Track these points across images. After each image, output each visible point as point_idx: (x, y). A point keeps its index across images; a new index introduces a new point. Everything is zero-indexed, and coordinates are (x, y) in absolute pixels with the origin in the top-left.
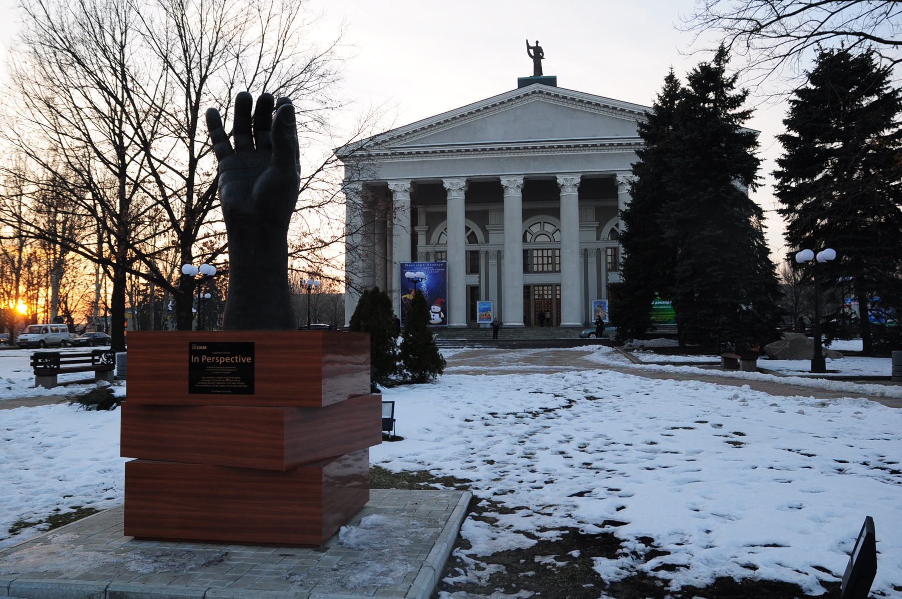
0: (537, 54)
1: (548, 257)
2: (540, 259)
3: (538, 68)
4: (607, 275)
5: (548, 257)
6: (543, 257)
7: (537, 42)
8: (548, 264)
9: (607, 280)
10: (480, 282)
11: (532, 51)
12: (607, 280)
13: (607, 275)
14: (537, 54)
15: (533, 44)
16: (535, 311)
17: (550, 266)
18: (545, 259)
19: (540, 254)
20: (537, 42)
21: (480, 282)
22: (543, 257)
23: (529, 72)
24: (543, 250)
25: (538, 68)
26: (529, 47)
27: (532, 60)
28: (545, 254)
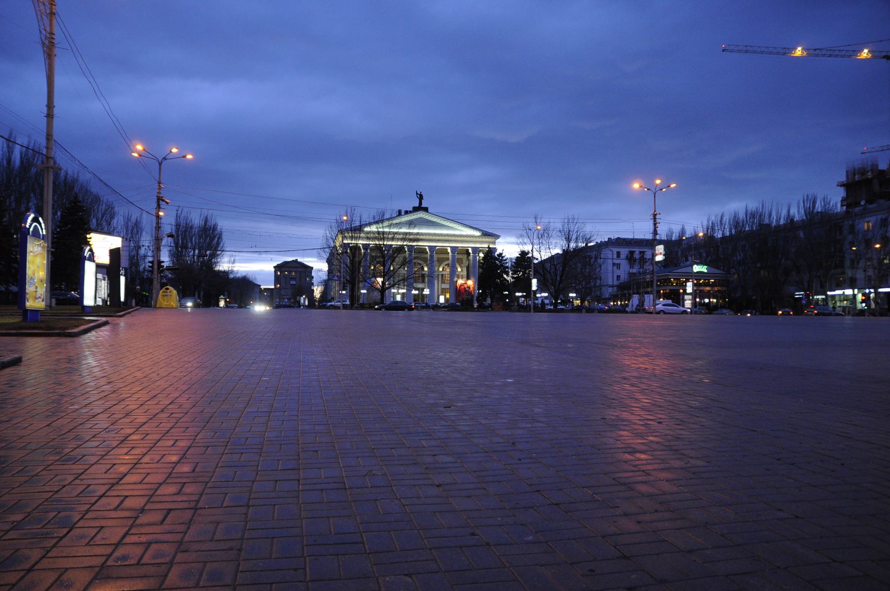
0: (421, 197)
3: (420, 203)
14: (421, 197)
23: (417, 205)
25: (420, 203)
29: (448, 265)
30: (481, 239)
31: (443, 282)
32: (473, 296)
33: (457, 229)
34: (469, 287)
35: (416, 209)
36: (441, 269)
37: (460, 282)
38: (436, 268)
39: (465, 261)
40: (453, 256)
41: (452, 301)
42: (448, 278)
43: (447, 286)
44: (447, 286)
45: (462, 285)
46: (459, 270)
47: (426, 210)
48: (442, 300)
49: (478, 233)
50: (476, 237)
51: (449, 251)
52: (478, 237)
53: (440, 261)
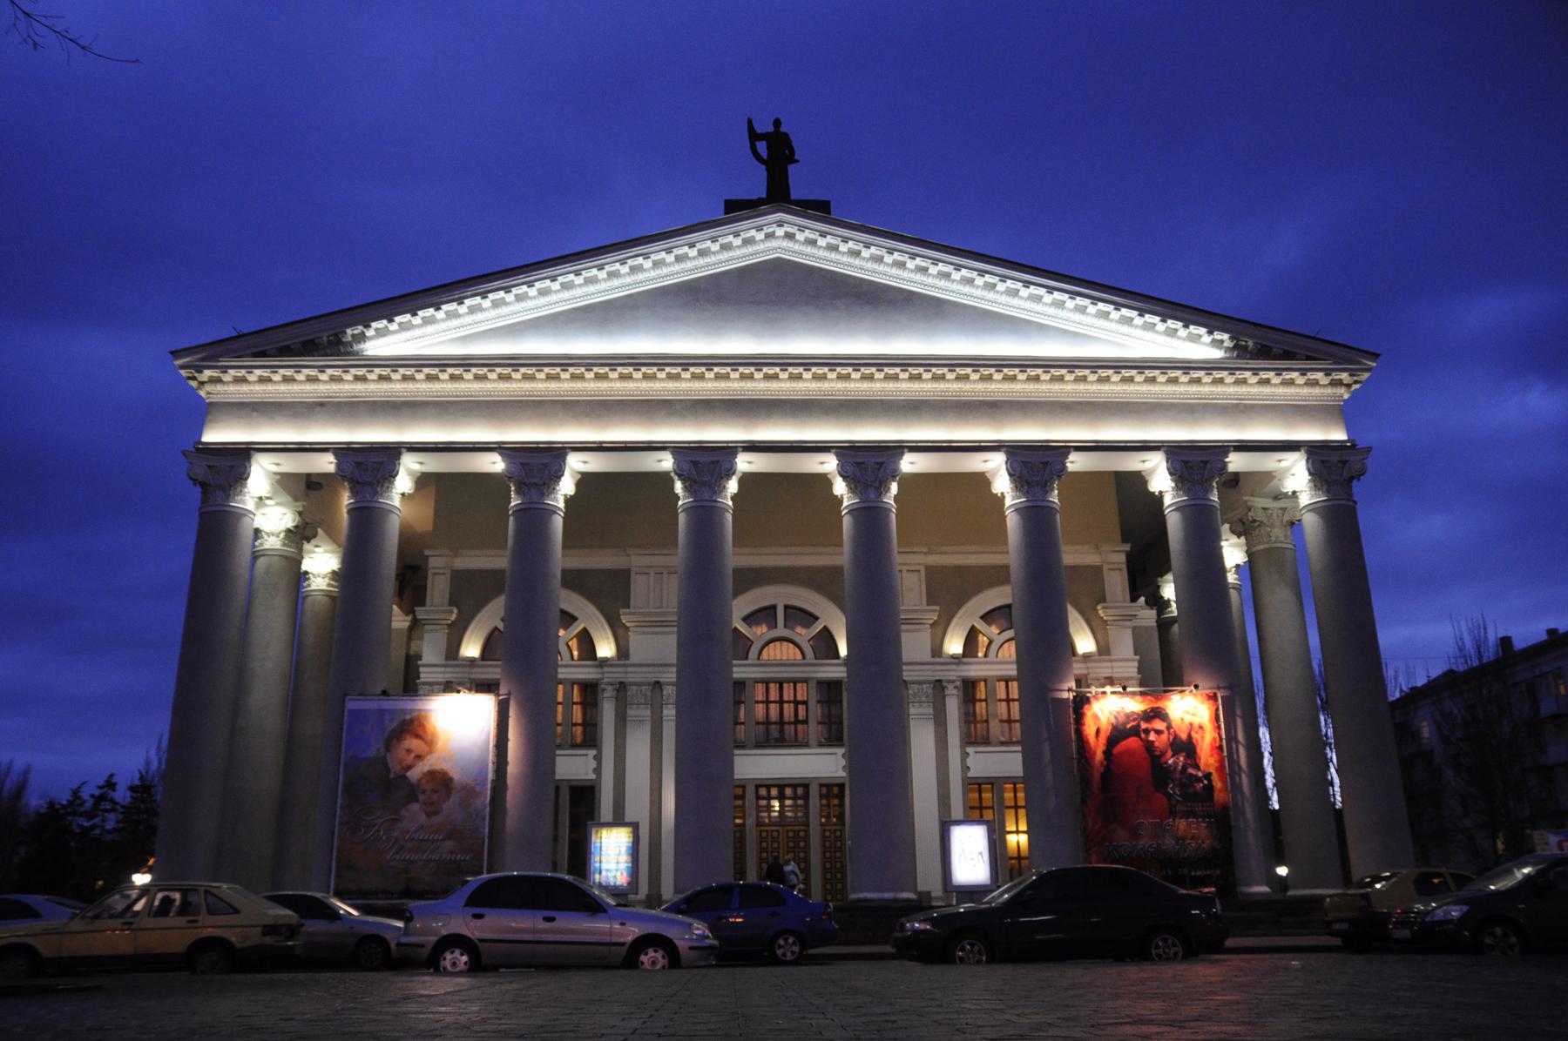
1: (796, 703)
2: (774, 708)
4: (965, 755)
5: (796, 703)
6: (781, 702)
7: (777, 123)
8: (797, 722)
9: (965, 768)
10: (598, 770)
11: (762, 147)
12: (965, 768)
13: (965, 755)
15: (764, 127)
16: (761, 860)
17: (800, 727)
18: (788, 710)
19: (774, 696)
20: (777, 123)
21: (598, 771)
22: (781, 702)
24: (781, 683)
26: (754, 136)
27: (762, 171)
28: (788, 694)
29: (987, 617)
30: (1229, 390)
31: (975, 737)
32: (1222, 821)
33: (1042, 329)
34: (1186, 746)
35: (738, 209)
36: (954, 645)
37: (1110, 707)
38: (914, 645)
39: (1117, 583)
40: (1037, 518)
41: (1067, 856)
42: (1004, 706)
43: (1006, 762)
44: (1006, 762)
45: (1119, 733)
46: (1085, 643)
47: (818, 209)
48: (970, 857)
49: (1200, 345)
50: (1186, 366)
51: (1002, 484)
52: (1209, 367)
53: (949, 591)
